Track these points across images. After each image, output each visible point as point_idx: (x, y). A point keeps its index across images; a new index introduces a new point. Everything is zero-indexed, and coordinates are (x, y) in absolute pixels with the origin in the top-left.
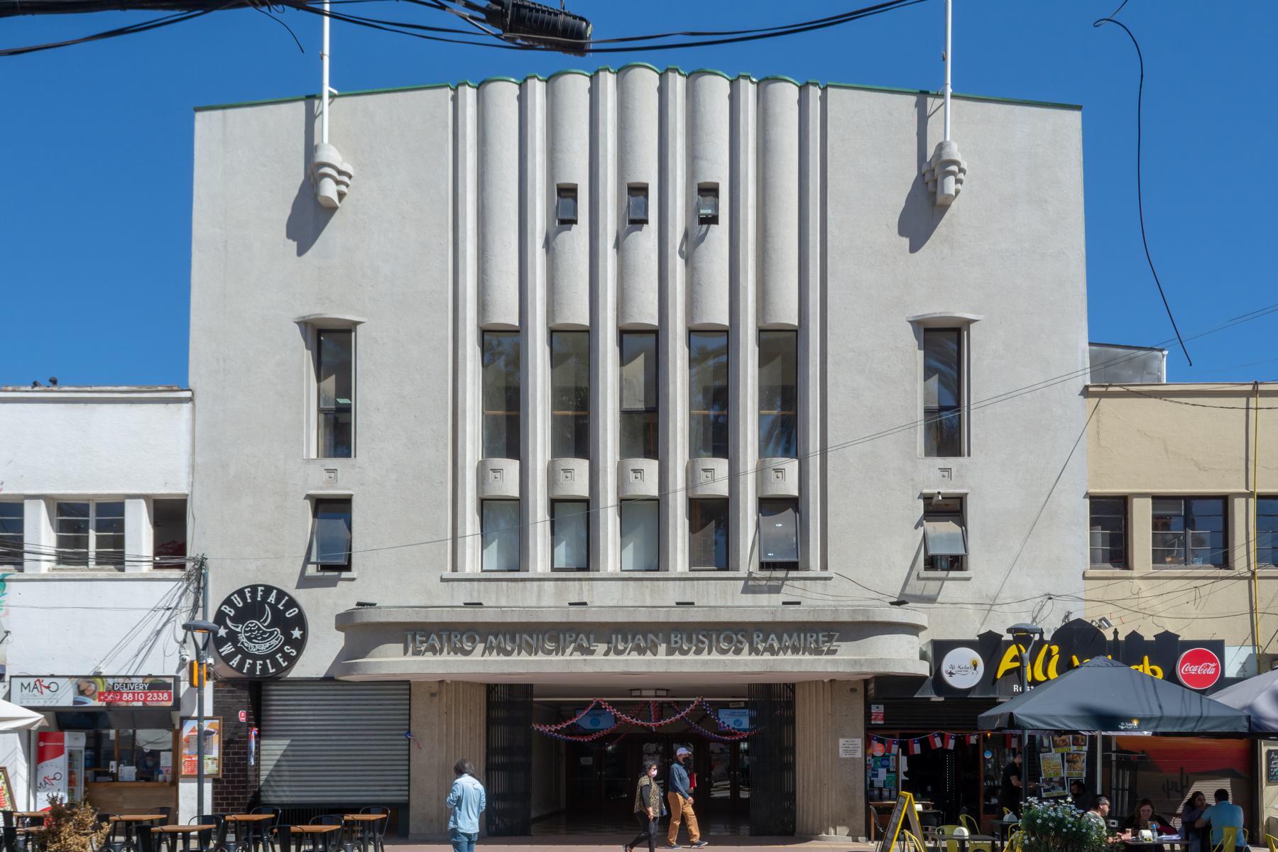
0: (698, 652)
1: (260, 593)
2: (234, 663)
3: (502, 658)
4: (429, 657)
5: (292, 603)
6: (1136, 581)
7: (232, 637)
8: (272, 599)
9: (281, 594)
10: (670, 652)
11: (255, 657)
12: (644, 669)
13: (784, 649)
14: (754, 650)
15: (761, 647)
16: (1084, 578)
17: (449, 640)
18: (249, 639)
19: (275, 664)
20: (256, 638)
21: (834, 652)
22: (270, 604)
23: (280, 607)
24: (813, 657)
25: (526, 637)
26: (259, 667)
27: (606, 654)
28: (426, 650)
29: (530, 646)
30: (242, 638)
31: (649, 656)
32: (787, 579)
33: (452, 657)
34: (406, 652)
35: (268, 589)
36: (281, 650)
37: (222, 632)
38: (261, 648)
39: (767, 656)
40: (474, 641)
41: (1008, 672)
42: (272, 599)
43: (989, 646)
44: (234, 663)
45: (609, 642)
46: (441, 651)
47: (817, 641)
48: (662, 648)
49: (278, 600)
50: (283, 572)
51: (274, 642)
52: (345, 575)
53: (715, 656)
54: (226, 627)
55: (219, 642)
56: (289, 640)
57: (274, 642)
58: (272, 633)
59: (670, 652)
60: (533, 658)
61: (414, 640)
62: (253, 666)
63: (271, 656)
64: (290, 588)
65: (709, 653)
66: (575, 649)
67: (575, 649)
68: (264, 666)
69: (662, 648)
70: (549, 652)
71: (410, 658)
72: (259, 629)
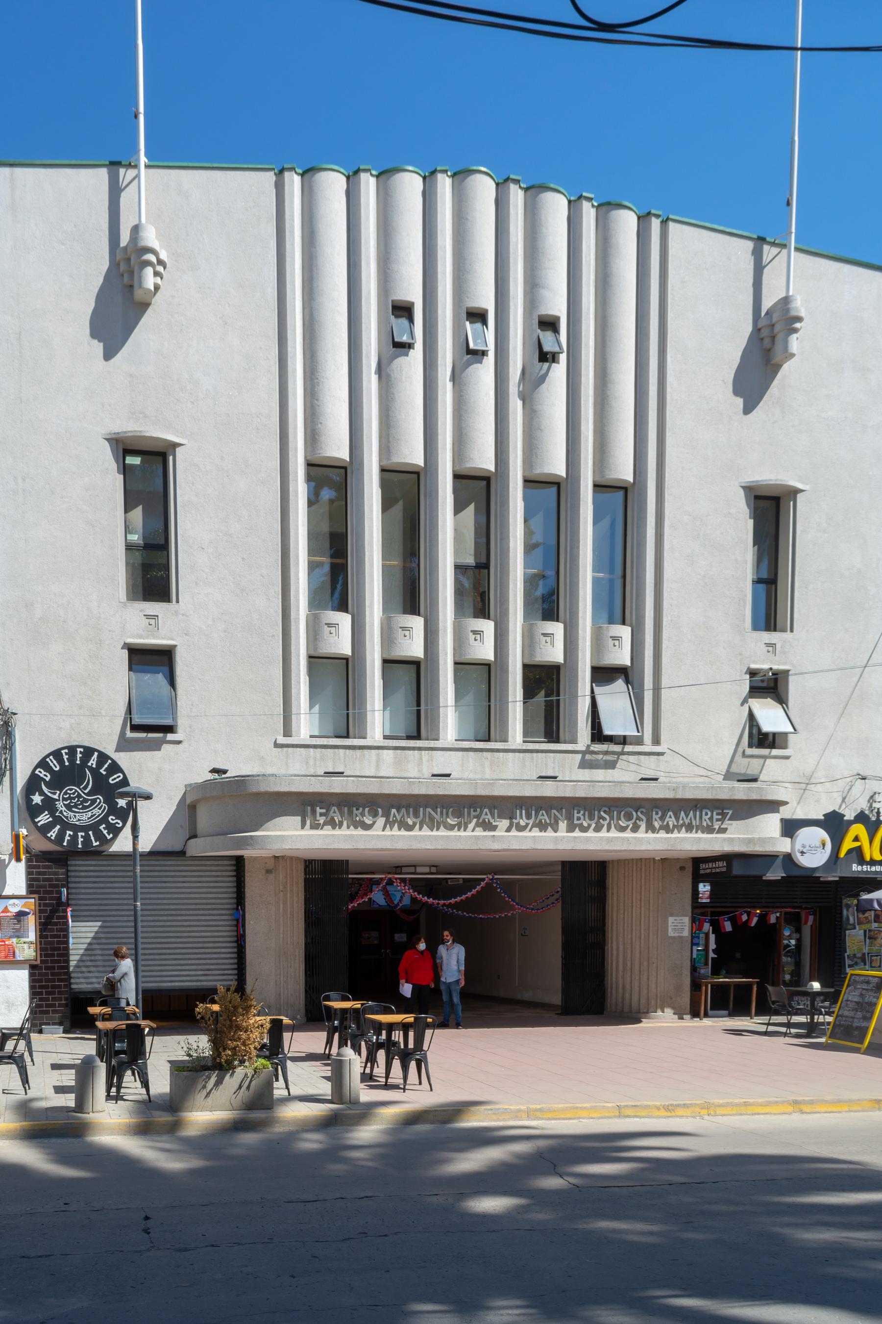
0: (598, 829)
2: (53, 834)
4: (328, 831)
5: (115, 768)
7: (49, 805)
8: (93, 762)
9: (103, 757)
10: (571, 828)
11: (76, 828)
12: (551, 846)
13: (678, 828)
14: (650, 828)
15: (656, 825)
17: (350, 813)
18: (69, 807)
19: (99, 836)
20: (76, 806)
21: (723, 831)
23: (103, 771)
24: (705, 836)
25: (429, 810)
26: (80, 840)
27: (508, 830)
28: (325, 824)
29: (432, 819)
30: (60, 806)
31: (550, 833)
33: (353, 832)
34: (303, 826)
35: (88, 752)
36: (105, 820)
37: (37, 799)
38: (82, 818)
39: (662, 834)
40: (375, 815)
41: (850, 851)
42: (93, 762)
43: (834, 824)
44: (53, 834)
45: (511, 818)
46: (341, 825)
47: (711, 819)
48: (563, 825)
49: (100, 764)
50: (103, 733)
51: (97, 811)
53: (614, 833)
54: (42, 793)
55: (33, 811)
56: (113, 809)
57: (97, 811)
58: (95, 800)
59: (571, 828)
60: (435, 833)
61: (314, 812)
62: (74, 838)
63: (94, 827)
64: (109, 749)
65: (608, 830)
66: (478, 825)
67: (478, 825)
68: (87, 838)
69: (563, 825)
70: (451, 828)
71: (308, 832)
72: (79, 796)
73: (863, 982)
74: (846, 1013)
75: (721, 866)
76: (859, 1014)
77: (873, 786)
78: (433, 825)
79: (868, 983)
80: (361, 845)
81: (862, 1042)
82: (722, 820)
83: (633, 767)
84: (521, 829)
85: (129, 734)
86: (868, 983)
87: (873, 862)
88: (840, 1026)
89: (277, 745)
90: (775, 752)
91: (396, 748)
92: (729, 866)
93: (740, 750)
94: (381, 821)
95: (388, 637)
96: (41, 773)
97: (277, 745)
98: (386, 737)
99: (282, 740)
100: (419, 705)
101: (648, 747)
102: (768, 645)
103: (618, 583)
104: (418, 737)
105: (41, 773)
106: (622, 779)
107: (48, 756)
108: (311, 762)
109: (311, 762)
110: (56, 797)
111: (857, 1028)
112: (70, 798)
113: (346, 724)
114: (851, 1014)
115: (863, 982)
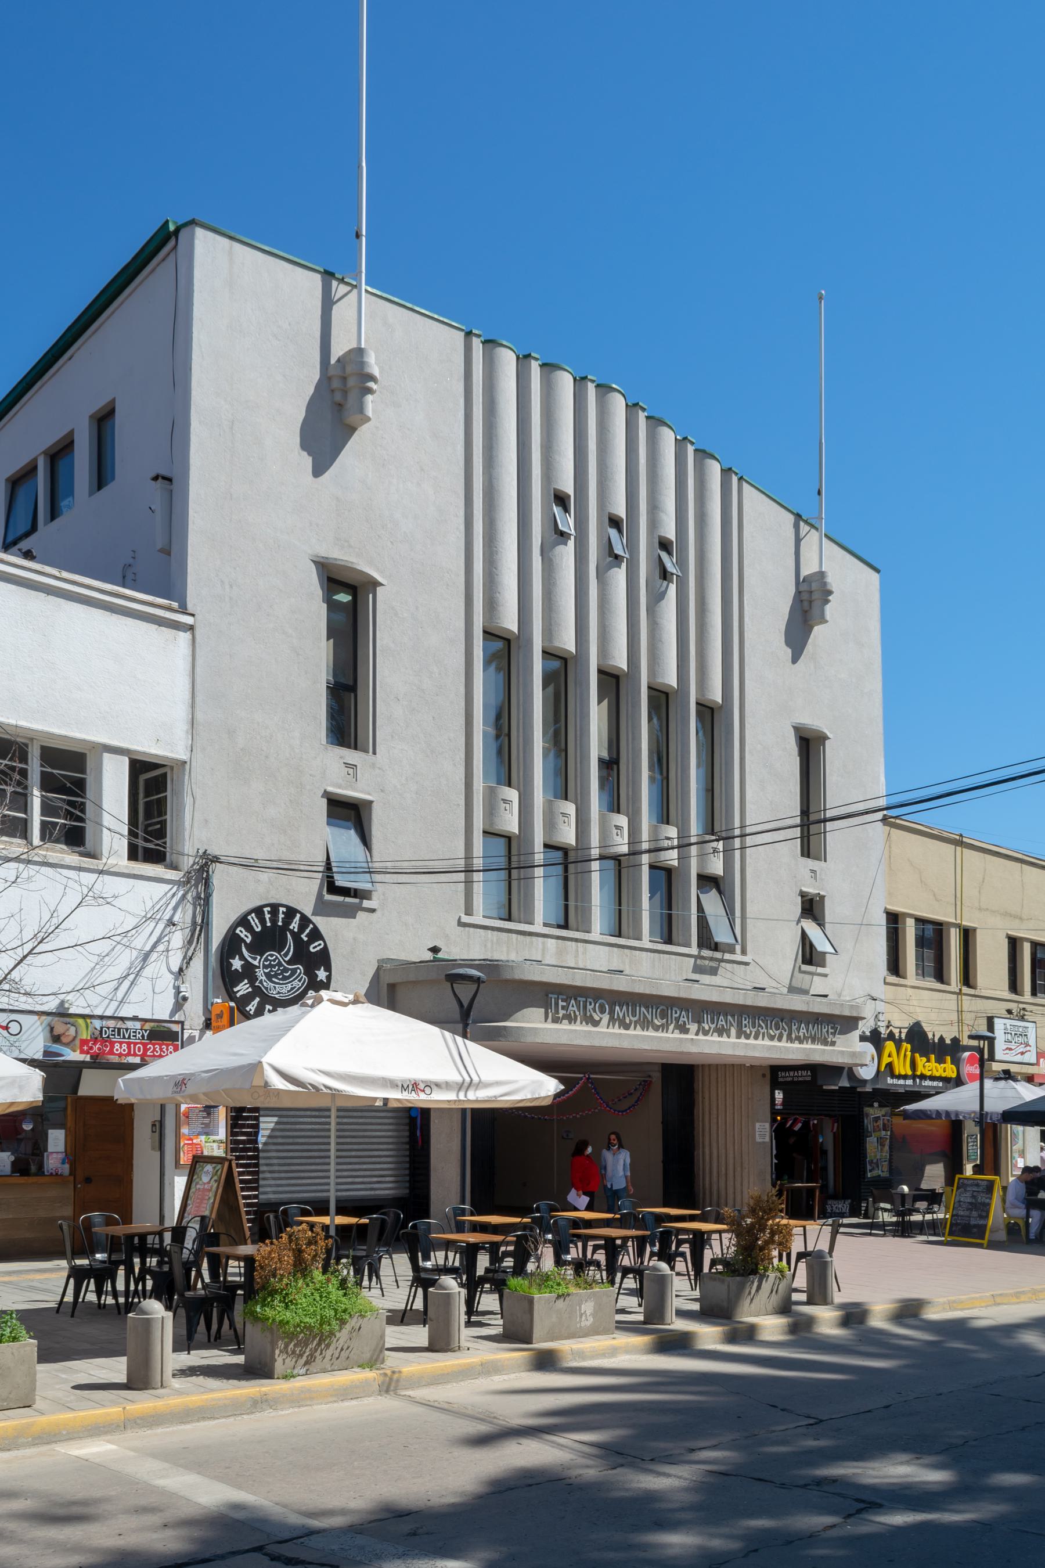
0: (756, 1038)
1: (281, 916)
3: (623, 1031)
5: (316, 935)
6: (909, 989)
7: (249, 971)
8: (295, 925)
9: (305, 921)
10: (738, 1037)
12: (730, 1052)
14: (790, 1039)
16: (885, 983)
18: (269, 976)
20: (276, 976)
21: (833, 1044)
22: (292, 932)
30: (260, 974)
32: (722, 960)
35: (291, 912)
42: (295, 925)
48: (733, 1031)
49: (302, 927)
50: (302, 893)
51: (297, 984)
52: (366, 904)
53: (767, 1042)
57: (297, 984)
58: (294, 971)
60: (645, 1033)
67: (676, 1027)
70: (656, 1028)
72: (280, 964)
73: (972, 1185)
74: (961, 1213)
75: (806, 1076)
76: (975, 1214)
77: (880, 1006)
78: (645, 1024)
79: (977, 1185)
80: (597, 1043)
81: (983, 1239)
82: (834, 1034)
83: (729, 975)
84: (706, 1033)
85: (328, 897)
86: (977, 1185)
87: (900, 1077)
88: (957, 1224)
89: (460, 924)
90: (820, 970)
91: (558, 938)
92: (814, 1076)
93: (797, 966)
94: (606, 1018)
95: (550, 824)
96: (242, 932)
97: (460, 924)
98: (545, 925)
99: (465, 919)
100: (620, 905)
101: (738, 957)
102: (812, 871)
103: (665, 781)
104: (565, 926)
105: (242, 932)
106: (724, 985)
107: (249, 913)
108: (489, 945)
109: (489, 945)
110: (256, 963)
111: (975, 1226)
112: (270, 966)
113: (512, 909)
114: (967, 1213)
115: (972, 1185)
